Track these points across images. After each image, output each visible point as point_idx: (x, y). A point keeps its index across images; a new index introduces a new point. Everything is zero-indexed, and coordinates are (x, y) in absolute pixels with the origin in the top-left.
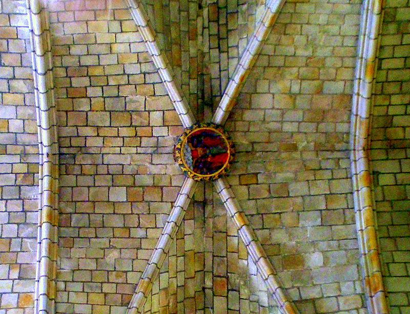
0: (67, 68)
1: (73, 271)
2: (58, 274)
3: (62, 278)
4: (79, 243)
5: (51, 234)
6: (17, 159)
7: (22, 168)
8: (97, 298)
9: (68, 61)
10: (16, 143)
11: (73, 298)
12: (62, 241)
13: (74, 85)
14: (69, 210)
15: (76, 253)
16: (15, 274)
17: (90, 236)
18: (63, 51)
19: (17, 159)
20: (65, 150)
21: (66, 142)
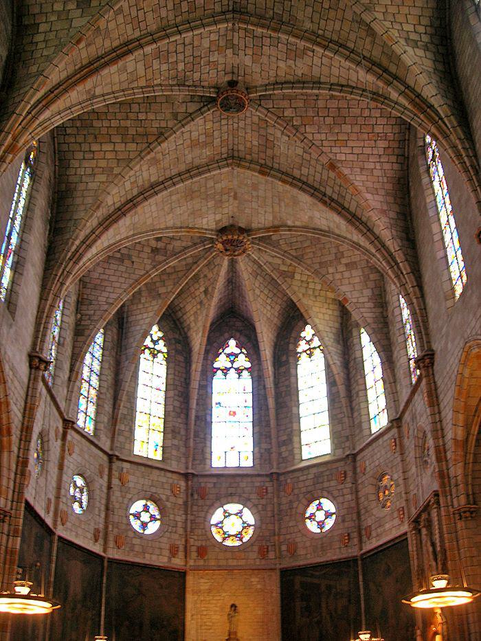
0: (176, 16)
1: (312, 22)
2: (313, 32)
3: (316, 30)
4: (294, 12)
5: (286, 33)
6: (236, 34)
7: (242, 33)
8: (332, 14)
9: (171, 16)
10: (226, 35)
11: (330, 28)
12: (291, 22)
13: (187, 10)
14: (271, 12)
15: (300, 16)
16: (311, 54)
17: (289, 5)
18: (165, 21)
19: (236, 34)
20: (231, 8)
21: (225, 8)
